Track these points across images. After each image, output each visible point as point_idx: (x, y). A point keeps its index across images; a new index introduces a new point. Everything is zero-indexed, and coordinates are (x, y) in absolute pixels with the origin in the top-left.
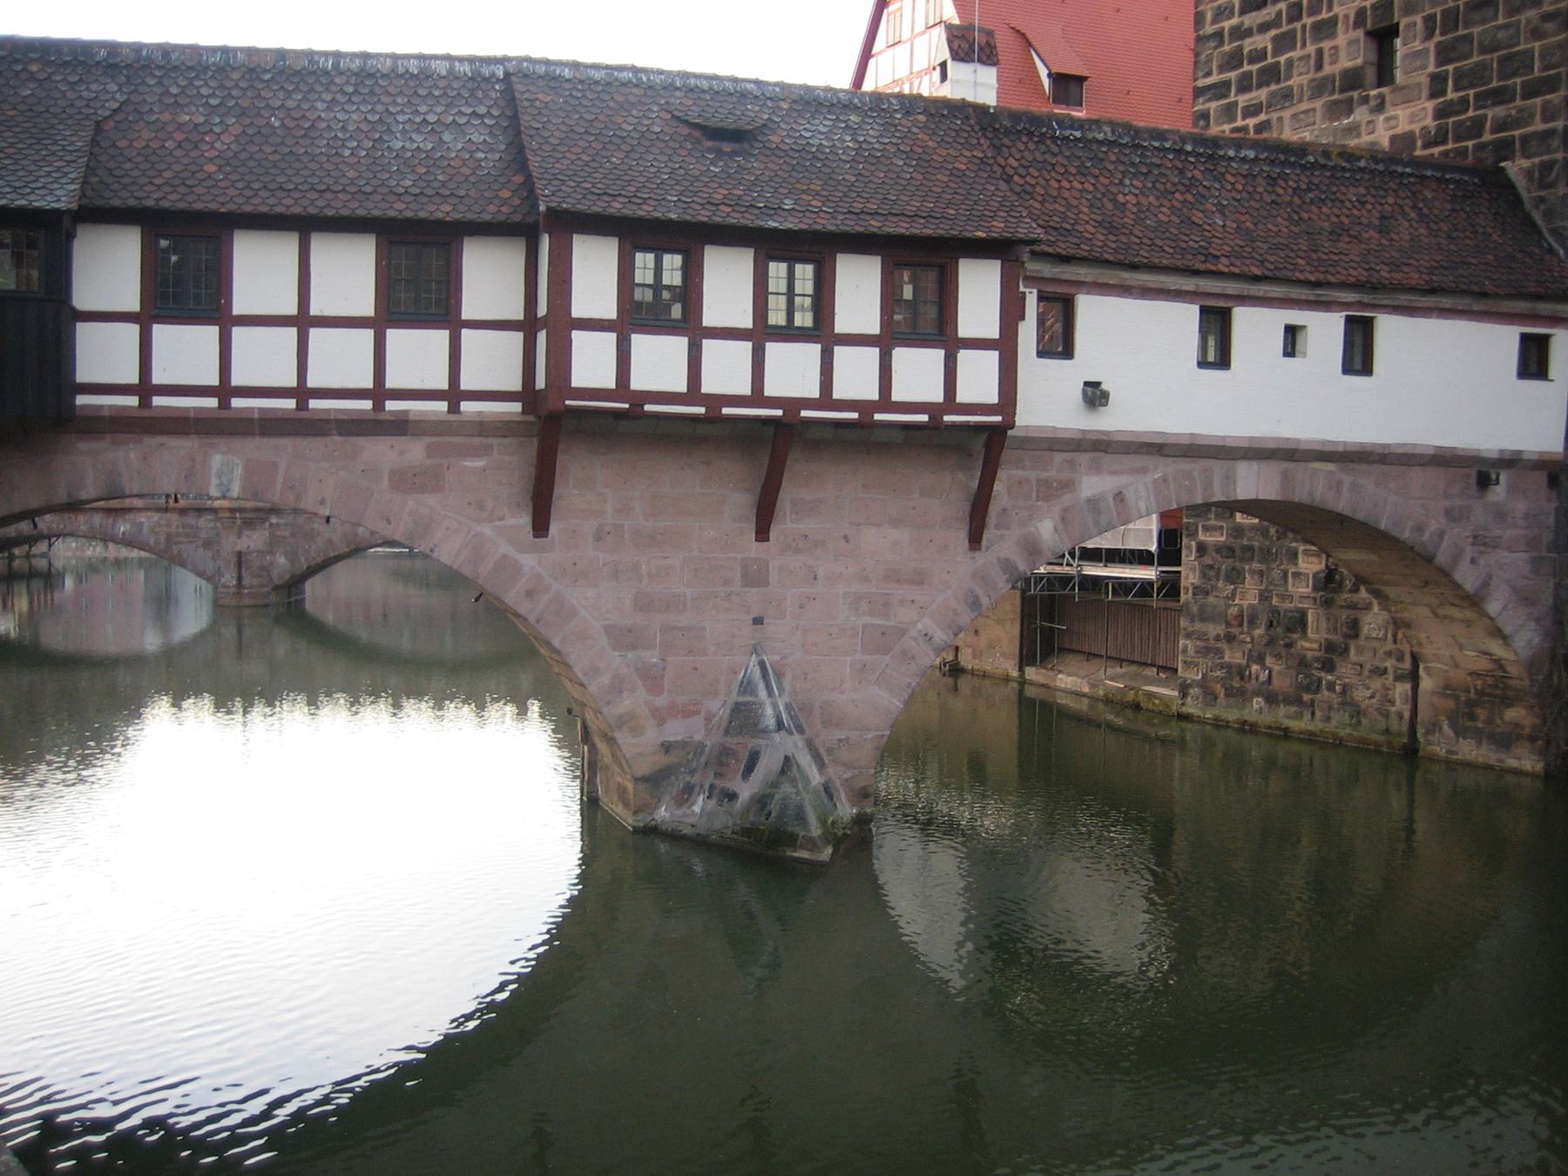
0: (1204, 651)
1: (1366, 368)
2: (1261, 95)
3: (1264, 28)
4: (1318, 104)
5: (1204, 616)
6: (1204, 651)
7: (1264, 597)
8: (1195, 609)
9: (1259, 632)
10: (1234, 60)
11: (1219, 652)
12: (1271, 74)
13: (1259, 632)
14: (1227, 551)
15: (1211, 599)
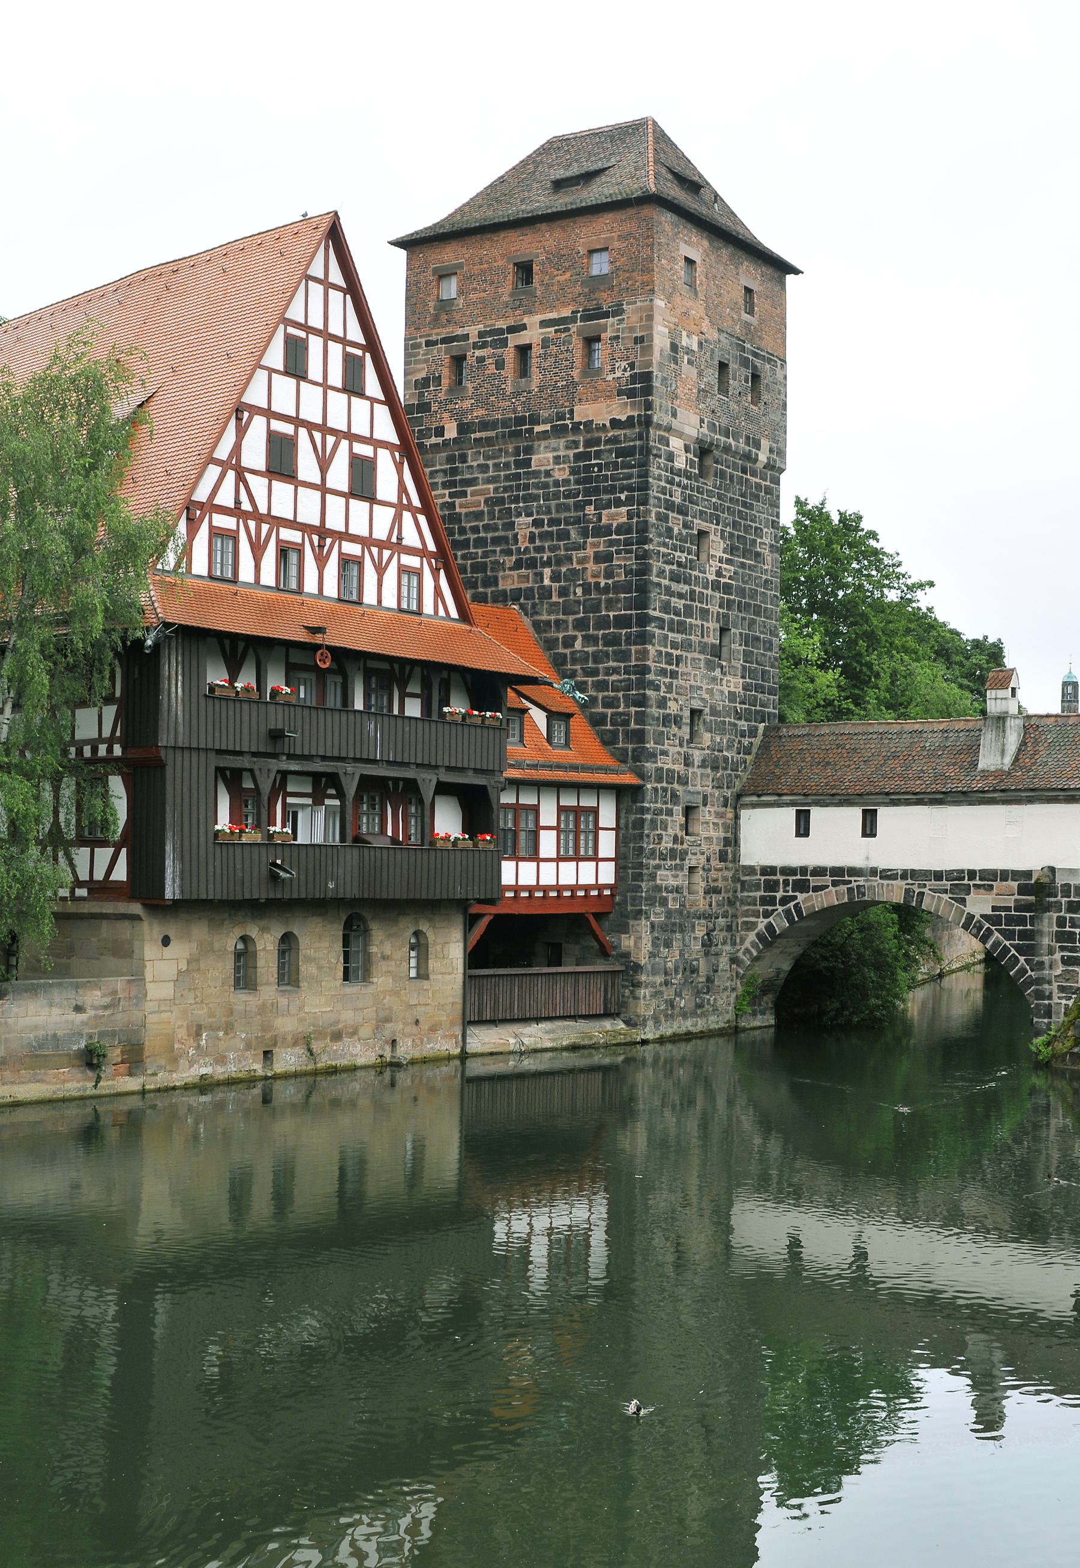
0: (655, 995)
1: (806, 834)
2: (678, 637)
3: (681, 596)
4: (702, 657)
5: (654, 972)
6: (655, 995)
7: (681, 955)
8: (649, 967)
9: (679, 976)
10: (666, 608)
11: (661, 993)
12: (681, 628)
13: (679, 976)
14: (664, 927)
15: (657, 959)
